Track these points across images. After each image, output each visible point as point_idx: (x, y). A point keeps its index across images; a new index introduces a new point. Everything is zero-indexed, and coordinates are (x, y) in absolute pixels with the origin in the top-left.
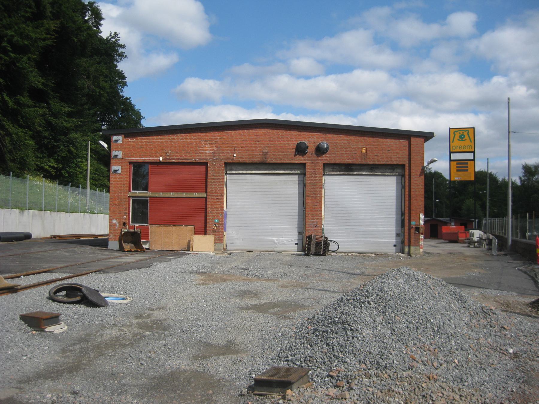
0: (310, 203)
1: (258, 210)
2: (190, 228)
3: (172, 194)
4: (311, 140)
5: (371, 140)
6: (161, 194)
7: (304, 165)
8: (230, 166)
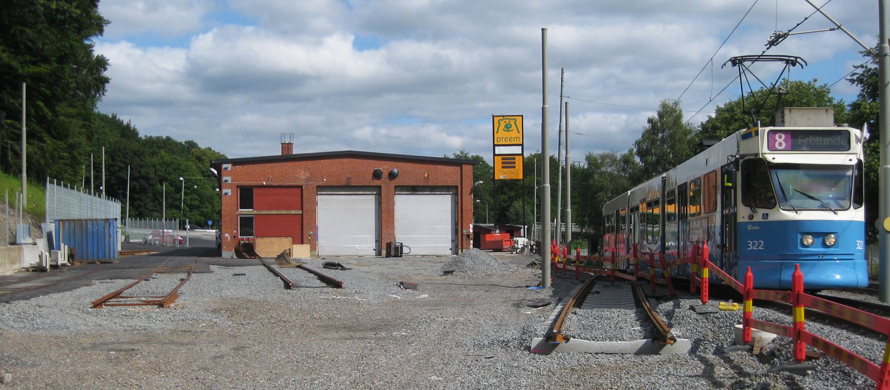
0: (384, 218)
1: (343, 225)
2: (290, 239)
3: (274, 212)
4: (385, 167)
5: (431, 167)
6: (265, 212)
7: (379, 187)
8: (321, 188)
